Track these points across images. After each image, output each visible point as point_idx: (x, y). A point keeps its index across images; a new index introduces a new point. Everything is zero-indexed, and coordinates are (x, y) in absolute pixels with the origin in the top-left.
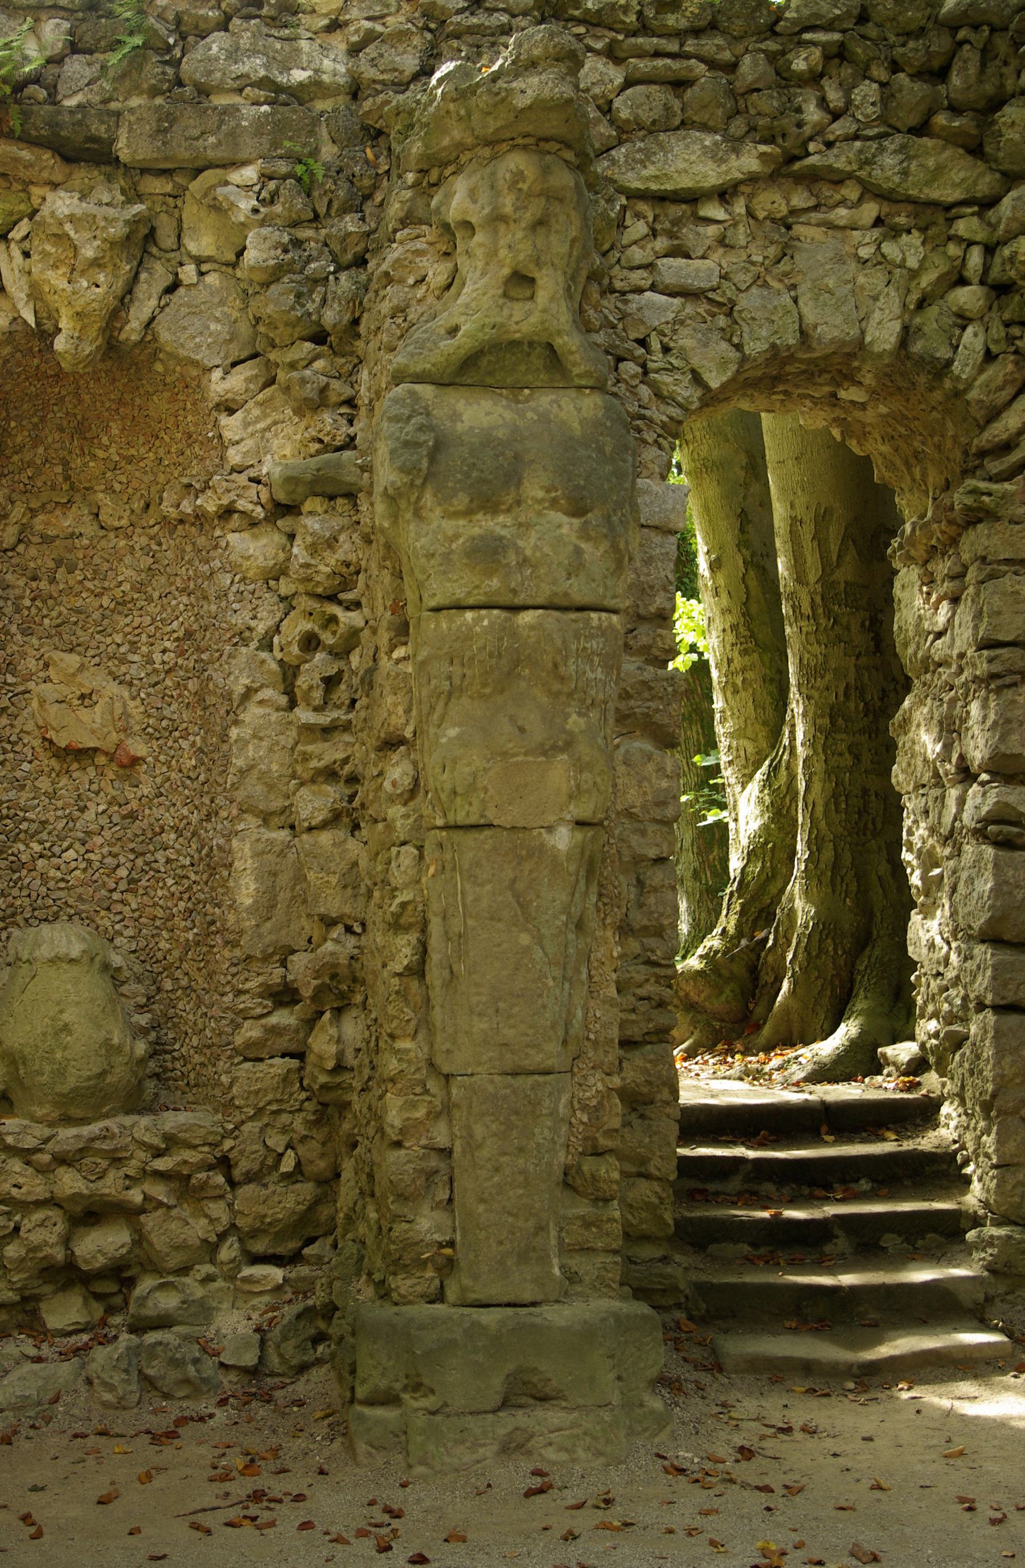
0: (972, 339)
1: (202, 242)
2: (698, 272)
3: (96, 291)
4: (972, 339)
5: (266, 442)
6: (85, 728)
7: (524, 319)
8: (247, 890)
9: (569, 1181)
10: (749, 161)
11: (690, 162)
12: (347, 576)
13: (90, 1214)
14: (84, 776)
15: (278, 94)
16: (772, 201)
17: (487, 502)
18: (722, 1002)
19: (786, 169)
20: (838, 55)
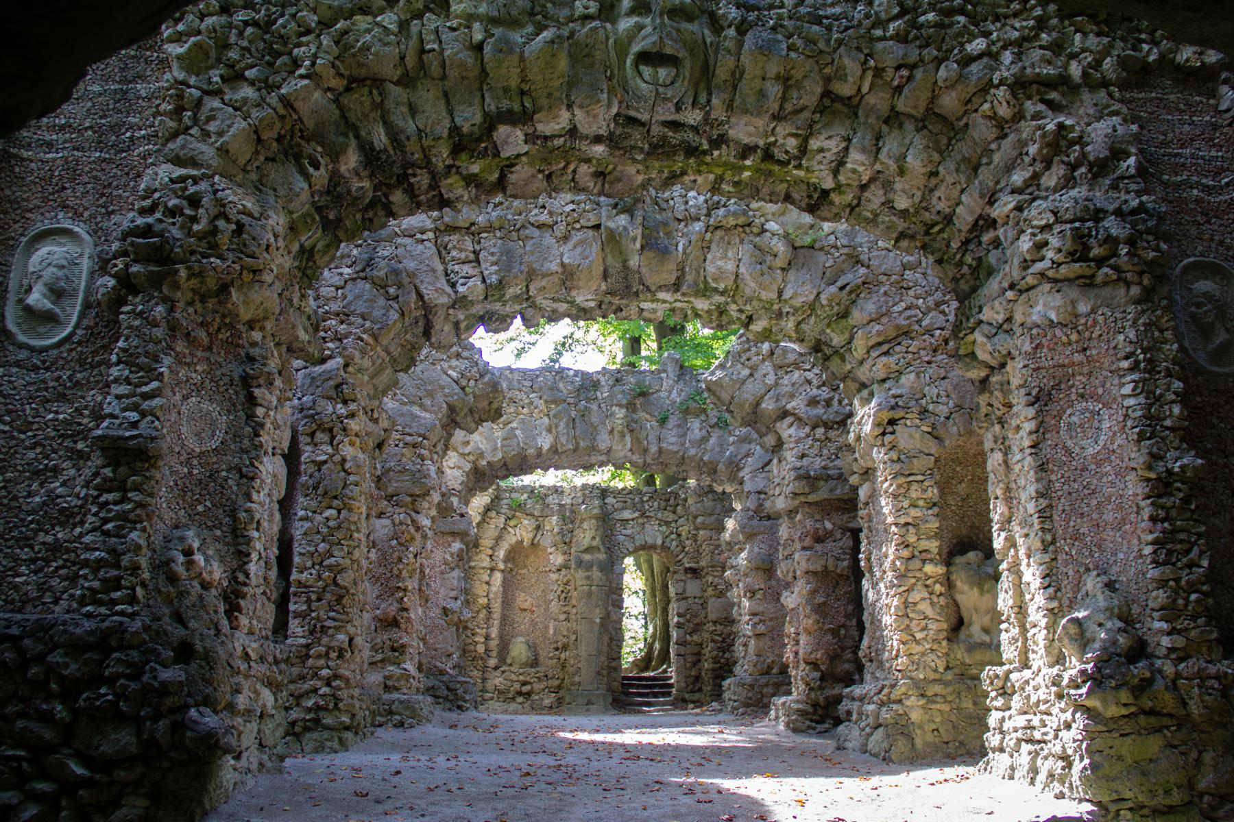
0: (674, 543)
1: (547, 528)
2: (629, 532)
3: (531, 535)
4: (674, 543)
5: (558, 559)
6: (526, 605)
7: (595, 543)
8: (551, 632)
9: (598, 673)
10: (636, 514)
11: (627, 514)
12: (568, 581)
13: (524, 684)
14: (525, 614)
15: (561, 506)
16: (641, 521)
17: (587, 570)
18: (643, 665)
19: (643, 515)
20: (651, 498)
